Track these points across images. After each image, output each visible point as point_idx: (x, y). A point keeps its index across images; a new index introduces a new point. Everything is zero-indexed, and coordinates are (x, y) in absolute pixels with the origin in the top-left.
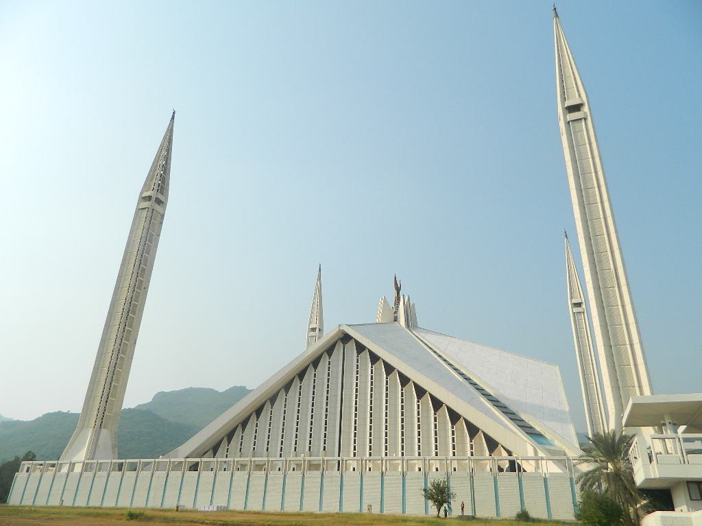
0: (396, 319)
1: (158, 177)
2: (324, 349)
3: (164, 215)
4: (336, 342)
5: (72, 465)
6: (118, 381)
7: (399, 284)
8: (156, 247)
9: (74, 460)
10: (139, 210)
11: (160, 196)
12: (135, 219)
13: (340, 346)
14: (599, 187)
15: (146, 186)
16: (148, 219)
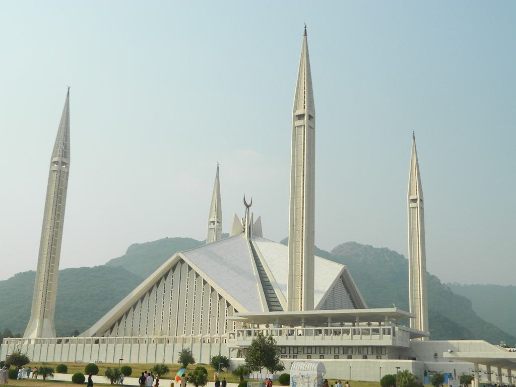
0: (244, 232)
1: (62, 143)
2: (171, 266)
3: (68, 173)
4: (177, 263)
5: (30, 341)
6: (50, 289)
7: (248, 203)
8: (65, 197)
9: (30, 338)
10: (52, 172)
11: (65, 160)
12: (49, 179)
13: (179, 264)
14: (304, 176)
15: (55, 152)
16: (58, 179)
